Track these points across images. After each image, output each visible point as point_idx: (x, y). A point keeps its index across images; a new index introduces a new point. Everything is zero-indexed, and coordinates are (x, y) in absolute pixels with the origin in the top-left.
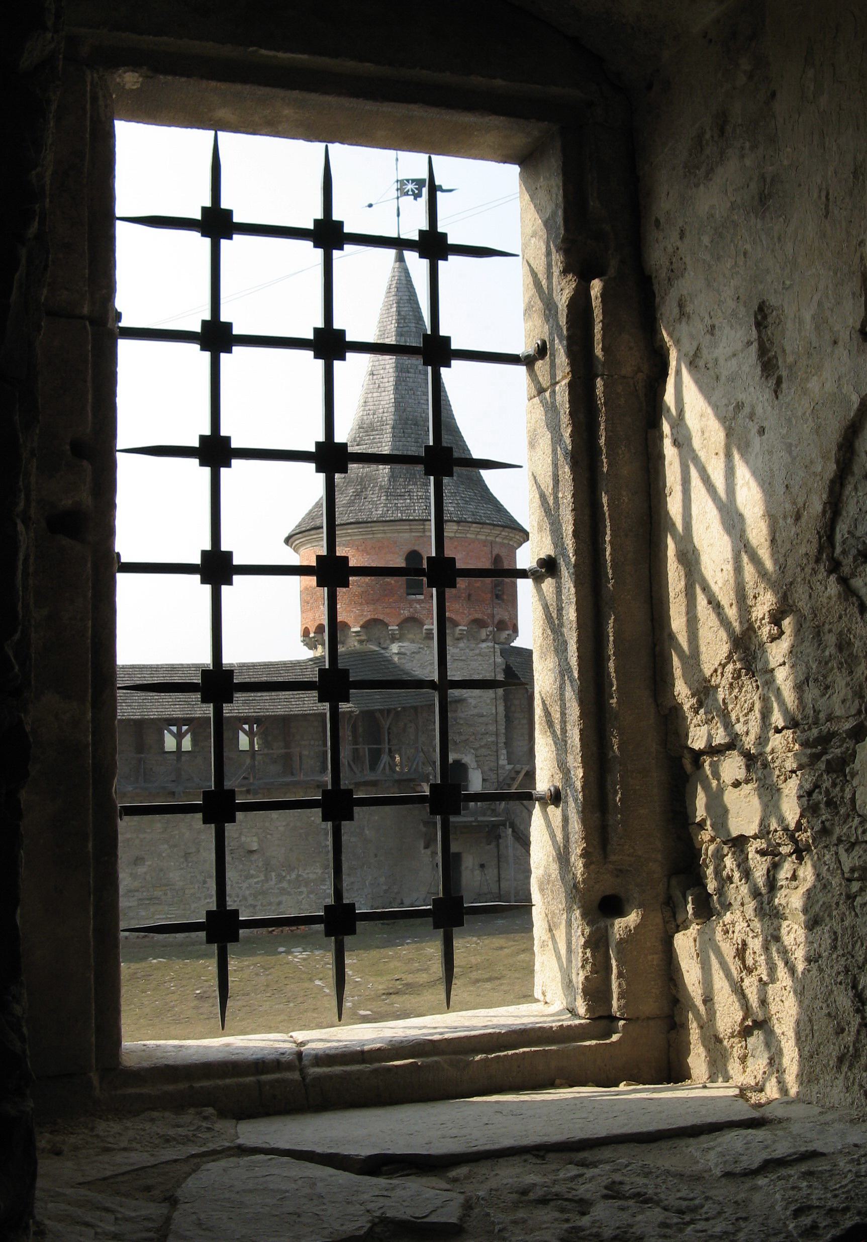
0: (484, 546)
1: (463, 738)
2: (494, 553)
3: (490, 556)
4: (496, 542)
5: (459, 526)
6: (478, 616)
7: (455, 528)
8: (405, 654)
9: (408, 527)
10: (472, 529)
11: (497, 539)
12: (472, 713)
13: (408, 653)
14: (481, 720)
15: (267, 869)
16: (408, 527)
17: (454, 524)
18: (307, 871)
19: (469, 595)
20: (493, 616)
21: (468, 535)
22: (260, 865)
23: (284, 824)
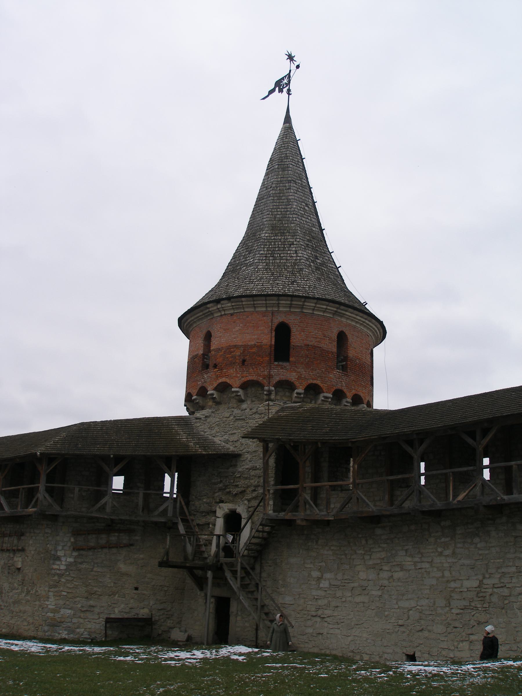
0: (264, 316)
1: (240, 490)
2: (276, 322)
3: (270, 324)
4: (278, 311)
5: (232, 302)
6: (250, 378)
7: (229, 305)
8: (200, 419)
9: (201, 314)
10: (244, 303)
11: (281, 309)
12: (247, 467)
13: (202, 417)
14: (253, 473)
15: (23, 583)
16: (201, 314)
17: (226, 302)
18: (41, 589)
19: (244, 361)
20: (270, 377)
21: (246, 310)
22: (20, 580)
23: (34, 548)
